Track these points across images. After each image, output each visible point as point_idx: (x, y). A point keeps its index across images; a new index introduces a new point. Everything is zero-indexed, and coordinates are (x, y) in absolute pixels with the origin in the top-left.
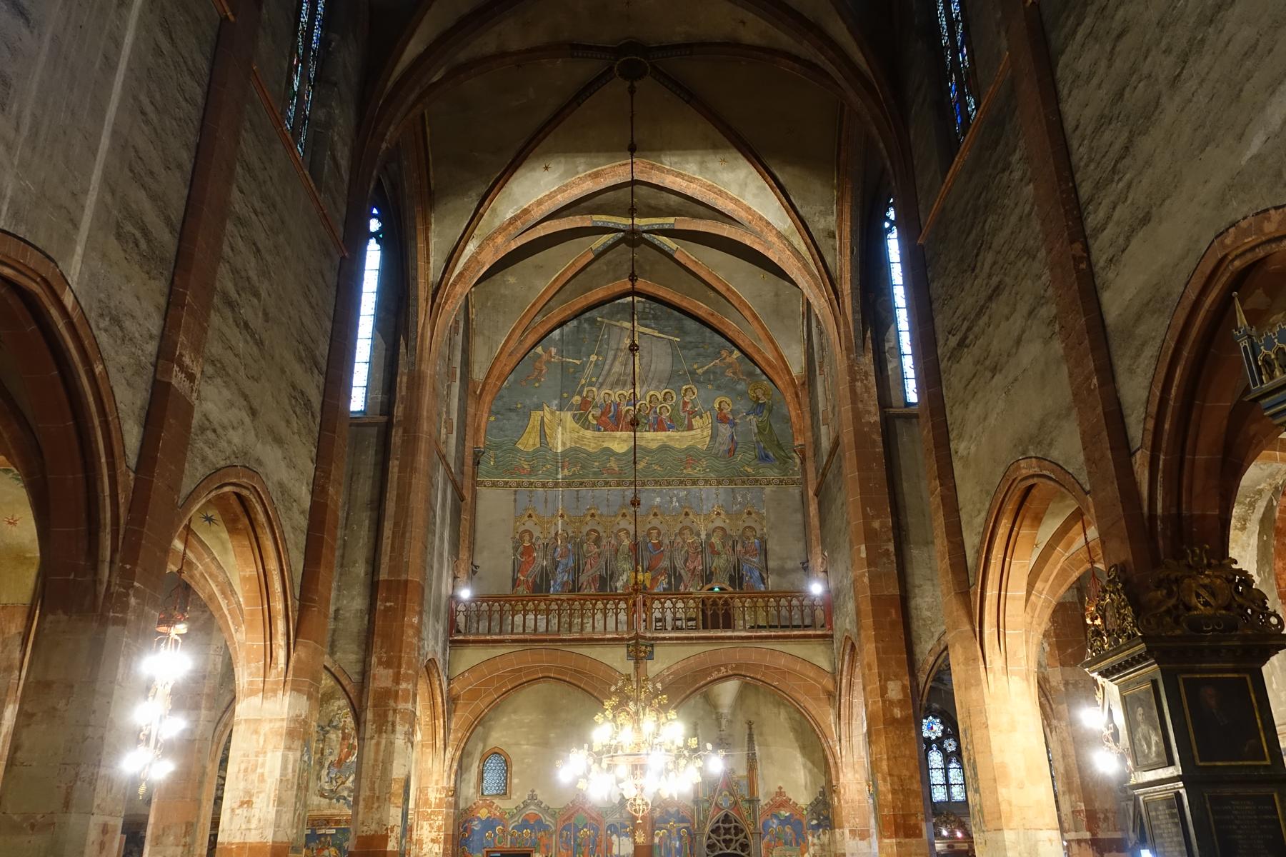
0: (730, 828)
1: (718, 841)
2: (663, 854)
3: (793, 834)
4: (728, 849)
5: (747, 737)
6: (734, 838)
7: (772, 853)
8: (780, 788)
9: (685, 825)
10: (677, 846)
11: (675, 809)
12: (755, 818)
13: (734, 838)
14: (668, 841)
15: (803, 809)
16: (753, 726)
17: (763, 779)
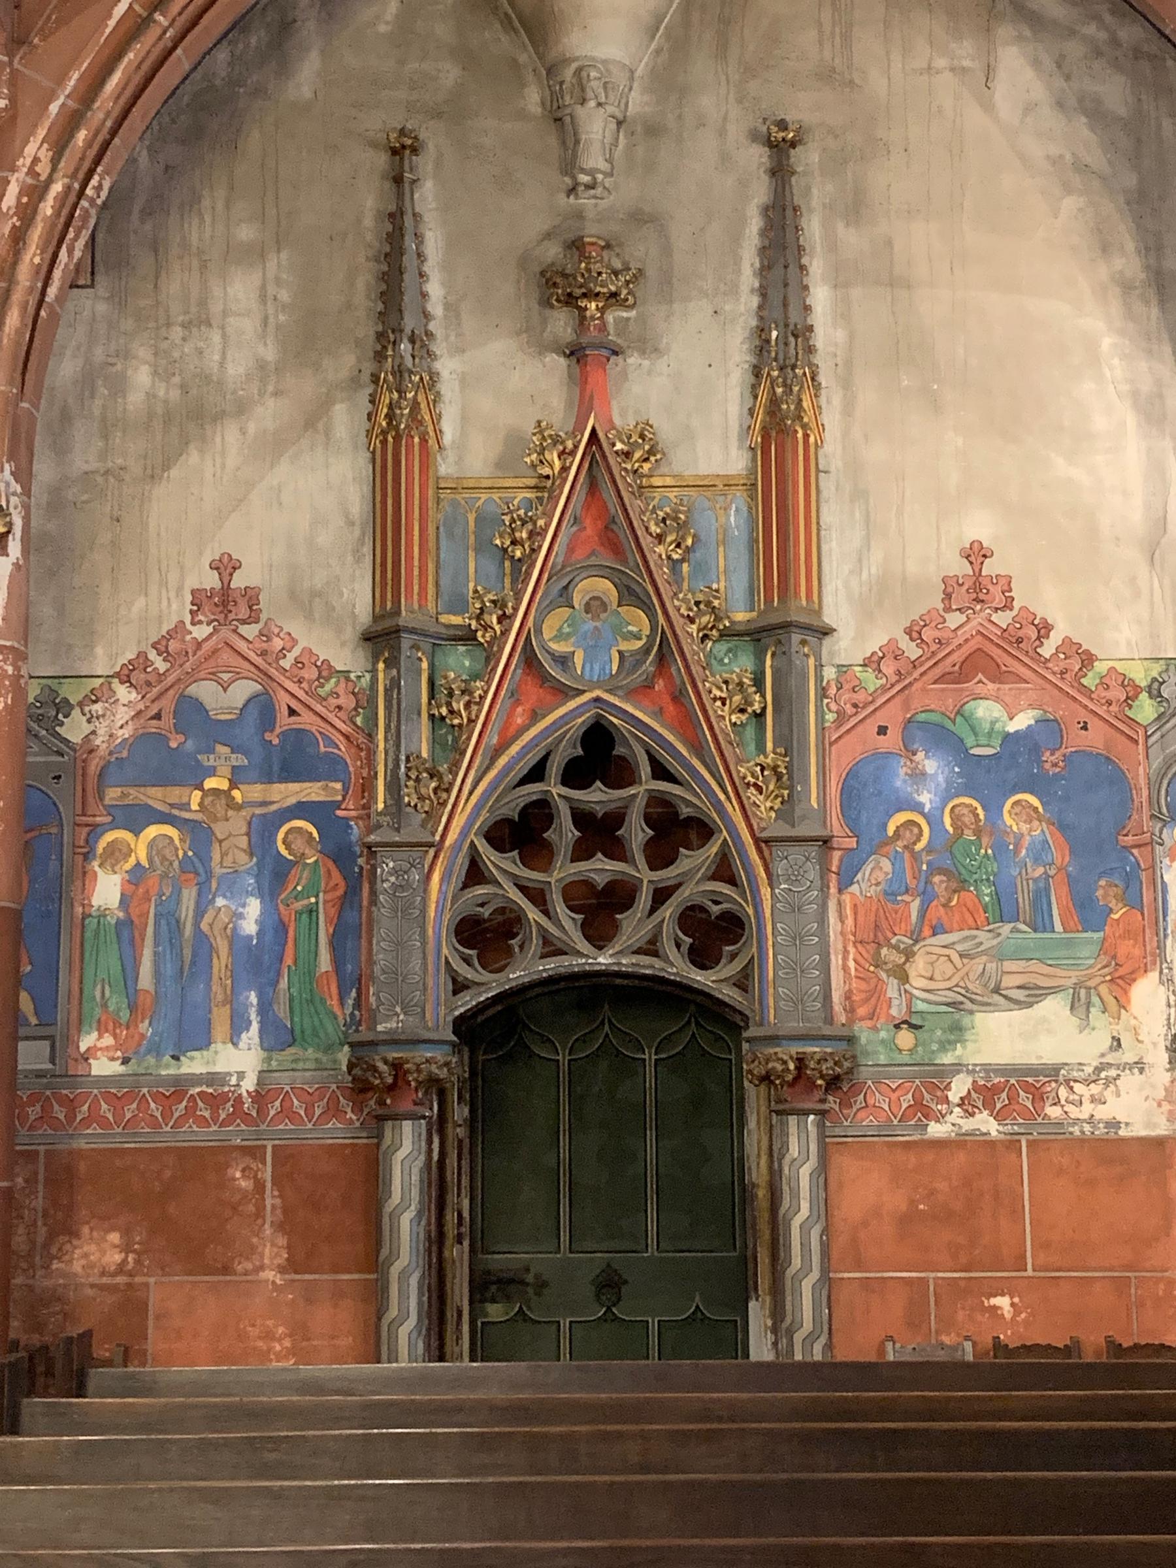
0: (616, 819)
1: (538, 897)
2: (146, 979)
3: (1059, 854)
4: (599, 933)
5: (755, 225)
6: (647, 878)
7: (904, 978)
8: (976, 554)
9: (313, 791)
10: (250, 927)
11: (243, 690)
12: (789, 742)
13: (647, 878)
14: (189, 896)
15: (1132, 692)
16: (806, 158)
17: (859, 495)
